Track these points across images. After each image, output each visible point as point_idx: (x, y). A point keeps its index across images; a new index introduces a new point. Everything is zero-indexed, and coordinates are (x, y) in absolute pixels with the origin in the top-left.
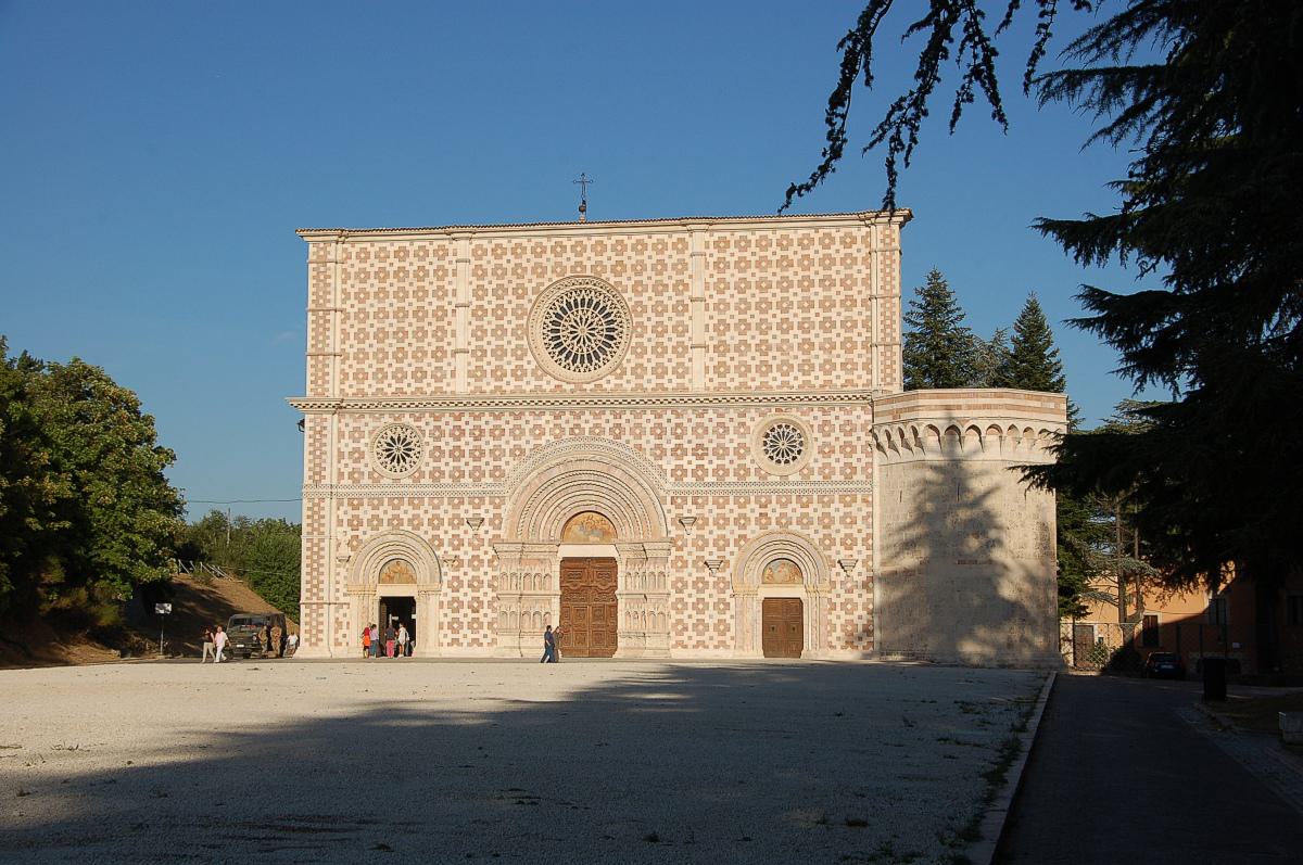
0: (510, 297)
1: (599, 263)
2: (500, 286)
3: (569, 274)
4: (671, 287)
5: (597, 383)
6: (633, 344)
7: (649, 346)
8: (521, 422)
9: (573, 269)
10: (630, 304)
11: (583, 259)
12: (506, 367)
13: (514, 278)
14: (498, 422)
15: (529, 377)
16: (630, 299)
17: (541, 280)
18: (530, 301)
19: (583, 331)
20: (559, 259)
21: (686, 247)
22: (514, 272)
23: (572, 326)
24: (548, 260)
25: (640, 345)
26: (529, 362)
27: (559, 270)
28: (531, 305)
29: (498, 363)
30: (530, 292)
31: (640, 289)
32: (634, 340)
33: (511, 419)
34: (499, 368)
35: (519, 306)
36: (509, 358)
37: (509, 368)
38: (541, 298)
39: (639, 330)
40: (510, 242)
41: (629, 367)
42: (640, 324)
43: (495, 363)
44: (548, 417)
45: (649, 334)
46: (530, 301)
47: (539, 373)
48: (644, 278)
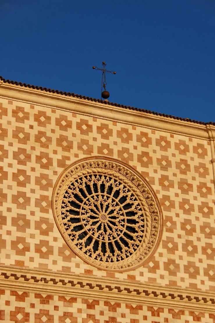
0: (33, 163)
1: (126, 150)
2: (23, 151)
3: (95, 153)
4: (195, 188)
5: (131, 273)
6: (164, 238)
7: (180, 242)
8: (50, 307)
9: (100, 150)
10: (160, 196)
11: (109, 142)
12: (28, 240)
13: (37, 145)
14: (21, 304)
15: (55, 256)
16: (158, 192)
17: (66, 154)
18: (55, 173)
19: (103, 217)
20: (85, 137)
21: (205, 153)
22: (38, 139)
23: (92, 211)
24: (74, 135)
25: (170, 240)
26: (55, 239)
27: (85, 147)
29: (20, 234)
30: (55, 163)
31: (166, 183)
32: (166, 235)
33: (37, 301)
34: (21, 240)
35: (43, 176)
36: (32, 230)
37: (32, 243)
38: (66, 173)
39: (169, 224)
40: (32, 107)
41: (162, 261)
42: (169, 219)
43: (16, 234)
44: (79, 304)
45: (178, 230)
47: (67, 253)
48: (169, 173)
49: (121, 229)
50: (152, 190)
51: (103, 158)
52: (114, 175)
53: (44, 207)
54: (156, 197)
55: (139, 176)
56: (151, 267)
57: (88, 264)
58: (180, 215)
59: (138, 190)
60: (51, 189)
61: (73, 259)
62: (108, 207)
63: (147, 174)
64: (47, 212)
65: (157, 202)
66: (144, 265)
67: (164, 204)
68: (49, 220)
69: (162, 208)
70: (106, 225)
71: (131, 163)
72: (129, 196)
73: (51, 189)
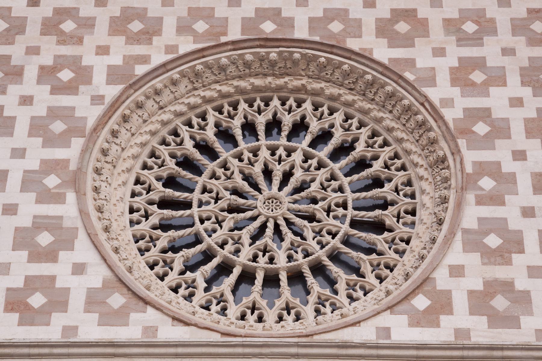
27: (201, 26)
28: (98, 111)
38: (138, 96)
46: (97, 99)
49: (334, 230)
50: (422, 100)
51: (257, 43)
52: (309, 87)
53: (50, 189)
54: (438, 117)
55: (380, 69)
56: (419, 311)
57: (187, 324)
58: (528, 153)
59: (387, 115)
60: (78, 143)
61: (134, 316)
62: (287, 176)
63: (411, 63)
64: (59, 199)
65: (444, 128)
66: (390, 308)
67: (467, 132)
68: (65, 220)
69: (462, 143)
70: (282, 222)
71: (353, 44)
72: (363, 138)
73: (78, 143)
